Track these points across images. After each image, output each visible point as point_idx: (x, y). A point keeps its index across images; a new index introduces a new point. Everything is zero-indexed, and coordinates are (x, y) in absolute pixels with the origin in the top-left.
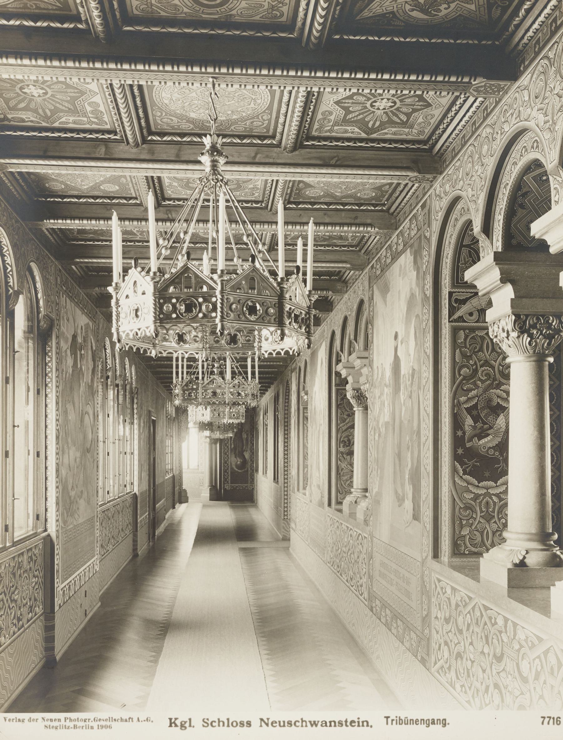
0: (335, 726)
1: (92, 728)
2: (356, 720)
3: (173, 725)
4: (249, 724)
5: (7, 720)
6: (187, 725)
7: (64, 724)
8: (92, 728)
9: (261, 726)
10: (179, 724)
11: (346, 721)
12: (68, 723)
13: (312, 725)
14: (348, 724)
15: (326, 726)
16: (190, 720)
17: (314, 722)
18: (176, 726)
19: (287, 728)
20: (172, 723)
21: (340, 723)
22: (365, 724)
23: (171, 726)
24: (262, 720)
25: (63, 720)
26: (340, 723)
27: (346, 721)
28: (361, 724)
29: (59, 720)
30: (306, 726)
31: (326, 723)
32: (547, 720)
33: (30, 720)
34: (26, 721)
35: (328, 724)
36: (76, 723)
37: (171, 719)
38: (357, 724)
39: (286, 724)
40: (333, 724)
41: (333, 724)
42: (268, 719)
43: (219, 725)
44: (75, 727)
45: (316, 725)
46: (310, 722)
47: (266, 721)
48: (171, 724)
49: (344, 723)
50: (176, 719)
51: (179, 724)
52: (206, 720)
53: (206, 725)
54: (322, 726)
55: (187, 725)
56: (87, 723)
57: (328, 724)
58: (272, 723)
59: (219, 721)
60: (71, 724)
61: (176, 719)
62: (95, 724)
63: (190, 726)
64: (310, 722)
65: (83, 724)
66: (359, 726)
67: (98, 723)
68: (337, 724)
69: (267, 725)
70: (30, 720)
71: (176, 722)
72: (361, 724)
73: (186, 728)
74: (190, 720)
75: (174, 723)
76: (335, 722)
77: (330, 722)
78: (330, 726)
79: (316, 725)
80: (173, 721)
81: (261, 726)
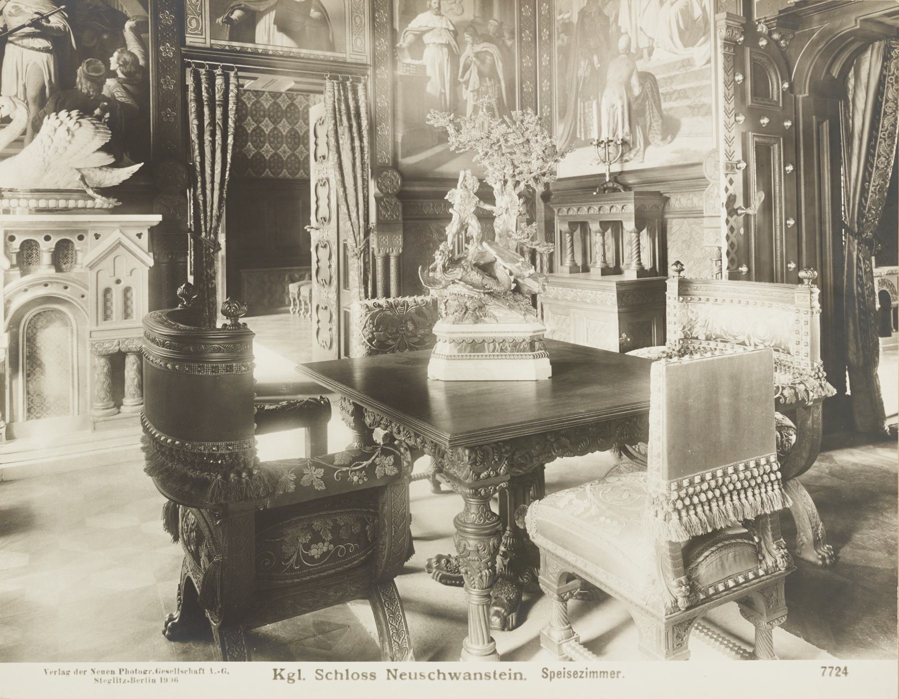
0: (481, 678)
1: (154, 681)
2: (507, 672)
3: (278, 677)
4: (373, 676)
5: (48, 672)
6: (296, 677)
7: (119, 676)
8: (154, 681)
9: (388, 679)
10: (286, 677)
11: (495, 673)
12: (124, 676)
13: (452, 678)
14: (497, 676)
15: (470, 678)
16: (299, 671)
17: (455, 674)
18: (282, 678)
19: (418, 680)
20: (277, 675)
21: (488, 676)
22: (518, 676)
23: (275, 678)
24: (389, 671)
25: (117, 672)
26: (488, 676)
27: (495, 673)
28: (513, 676)
29: (113, 672)
30: (444, 679)
31: (470, 675)
32: (828, 670)
33: (76, 672)
34: (71, 673)
35: (472, 677)
36: (134, 675)
37: (275, 670)
38: (508, 676)
39: (418, 676)
40: (478, 676)
41: (478, 676)
42: (396, 670)
43: (336, 678)
44: (133, 680)
45: (458, 679)
46: (450, 674)
47: (394, 672)
48: (276, 675)
49: (492, 675)
50: (282, 670)
51: (286, 677)
52: (319, 672)
53: (320, 677)
54: (464, 678)
55: (296, 677)
56: (147, 676)
57: (472, 677)
58: (401, 675)
59: (336, 673)
60: (128, 677)
61: (282, 670)
62: (157, 677)
63: (300, 678)
64: (450, 674)
65: (143, 676)
66: (510, 678)
67: (161, 675)
68: (483, 676)
69: (395, 677)
70: (76, 672)
71: (283, 673)
72: (513, 676)
73: (294, 681)
74: (299, 671)
75: (280, 674)
76: (481, 674)
77: (475, 674)
78: (475, 679)
79: (458, 679)
80: (278, 672)
81: (388, 679)
